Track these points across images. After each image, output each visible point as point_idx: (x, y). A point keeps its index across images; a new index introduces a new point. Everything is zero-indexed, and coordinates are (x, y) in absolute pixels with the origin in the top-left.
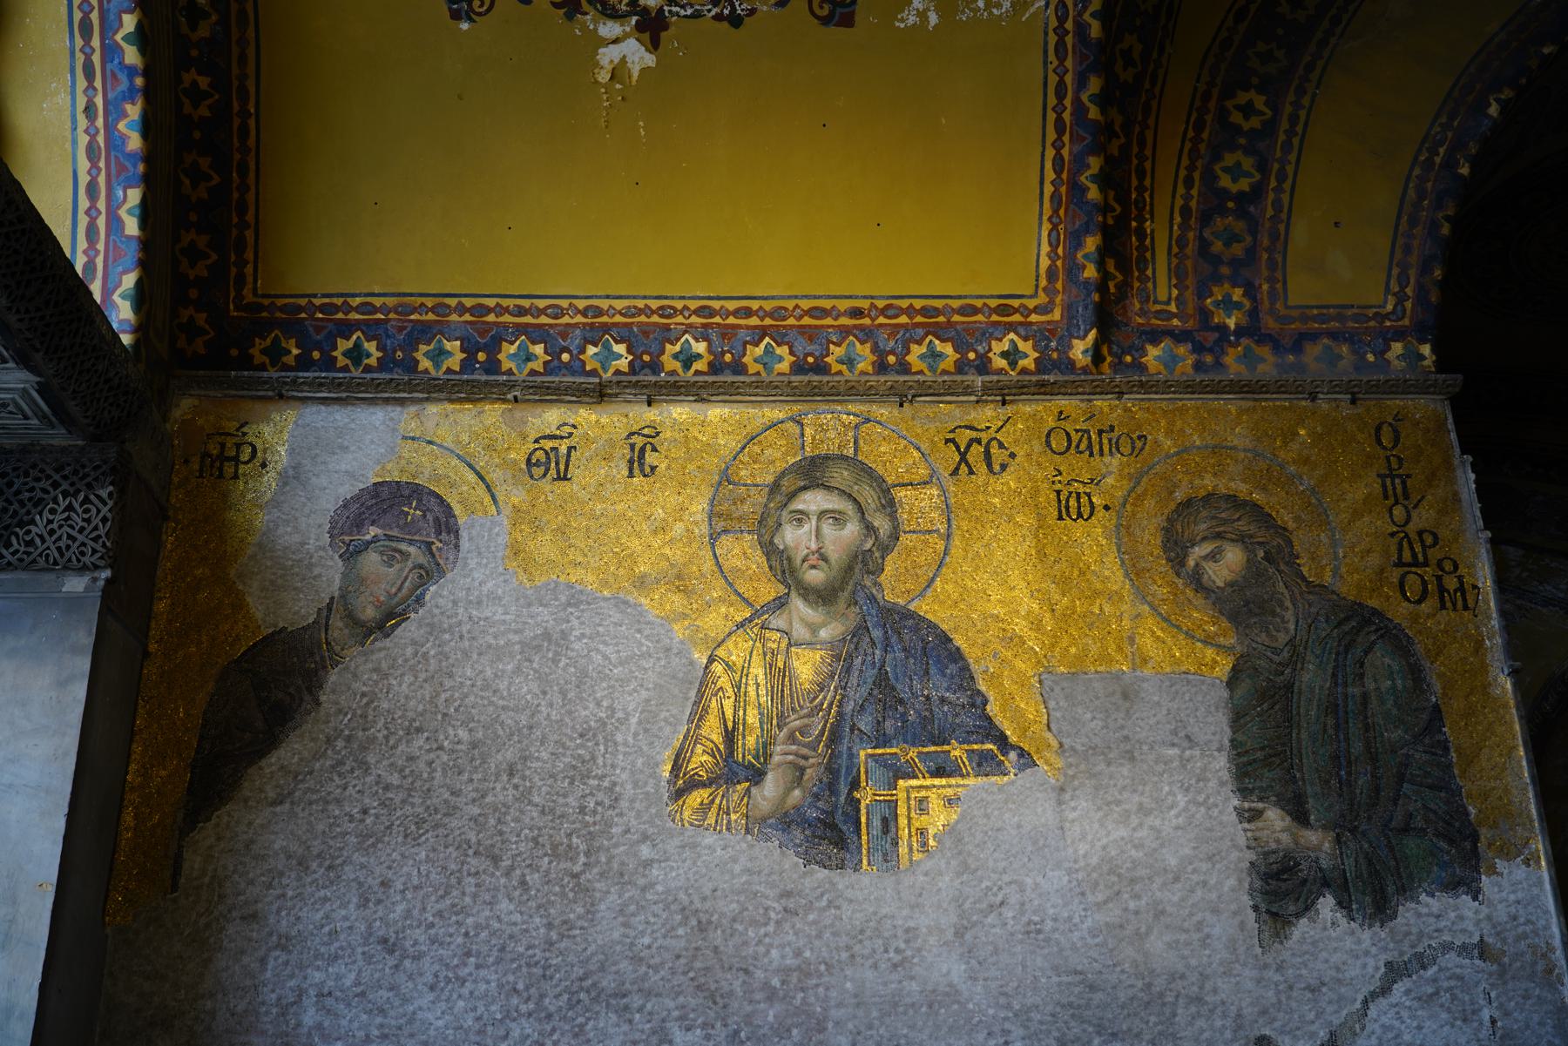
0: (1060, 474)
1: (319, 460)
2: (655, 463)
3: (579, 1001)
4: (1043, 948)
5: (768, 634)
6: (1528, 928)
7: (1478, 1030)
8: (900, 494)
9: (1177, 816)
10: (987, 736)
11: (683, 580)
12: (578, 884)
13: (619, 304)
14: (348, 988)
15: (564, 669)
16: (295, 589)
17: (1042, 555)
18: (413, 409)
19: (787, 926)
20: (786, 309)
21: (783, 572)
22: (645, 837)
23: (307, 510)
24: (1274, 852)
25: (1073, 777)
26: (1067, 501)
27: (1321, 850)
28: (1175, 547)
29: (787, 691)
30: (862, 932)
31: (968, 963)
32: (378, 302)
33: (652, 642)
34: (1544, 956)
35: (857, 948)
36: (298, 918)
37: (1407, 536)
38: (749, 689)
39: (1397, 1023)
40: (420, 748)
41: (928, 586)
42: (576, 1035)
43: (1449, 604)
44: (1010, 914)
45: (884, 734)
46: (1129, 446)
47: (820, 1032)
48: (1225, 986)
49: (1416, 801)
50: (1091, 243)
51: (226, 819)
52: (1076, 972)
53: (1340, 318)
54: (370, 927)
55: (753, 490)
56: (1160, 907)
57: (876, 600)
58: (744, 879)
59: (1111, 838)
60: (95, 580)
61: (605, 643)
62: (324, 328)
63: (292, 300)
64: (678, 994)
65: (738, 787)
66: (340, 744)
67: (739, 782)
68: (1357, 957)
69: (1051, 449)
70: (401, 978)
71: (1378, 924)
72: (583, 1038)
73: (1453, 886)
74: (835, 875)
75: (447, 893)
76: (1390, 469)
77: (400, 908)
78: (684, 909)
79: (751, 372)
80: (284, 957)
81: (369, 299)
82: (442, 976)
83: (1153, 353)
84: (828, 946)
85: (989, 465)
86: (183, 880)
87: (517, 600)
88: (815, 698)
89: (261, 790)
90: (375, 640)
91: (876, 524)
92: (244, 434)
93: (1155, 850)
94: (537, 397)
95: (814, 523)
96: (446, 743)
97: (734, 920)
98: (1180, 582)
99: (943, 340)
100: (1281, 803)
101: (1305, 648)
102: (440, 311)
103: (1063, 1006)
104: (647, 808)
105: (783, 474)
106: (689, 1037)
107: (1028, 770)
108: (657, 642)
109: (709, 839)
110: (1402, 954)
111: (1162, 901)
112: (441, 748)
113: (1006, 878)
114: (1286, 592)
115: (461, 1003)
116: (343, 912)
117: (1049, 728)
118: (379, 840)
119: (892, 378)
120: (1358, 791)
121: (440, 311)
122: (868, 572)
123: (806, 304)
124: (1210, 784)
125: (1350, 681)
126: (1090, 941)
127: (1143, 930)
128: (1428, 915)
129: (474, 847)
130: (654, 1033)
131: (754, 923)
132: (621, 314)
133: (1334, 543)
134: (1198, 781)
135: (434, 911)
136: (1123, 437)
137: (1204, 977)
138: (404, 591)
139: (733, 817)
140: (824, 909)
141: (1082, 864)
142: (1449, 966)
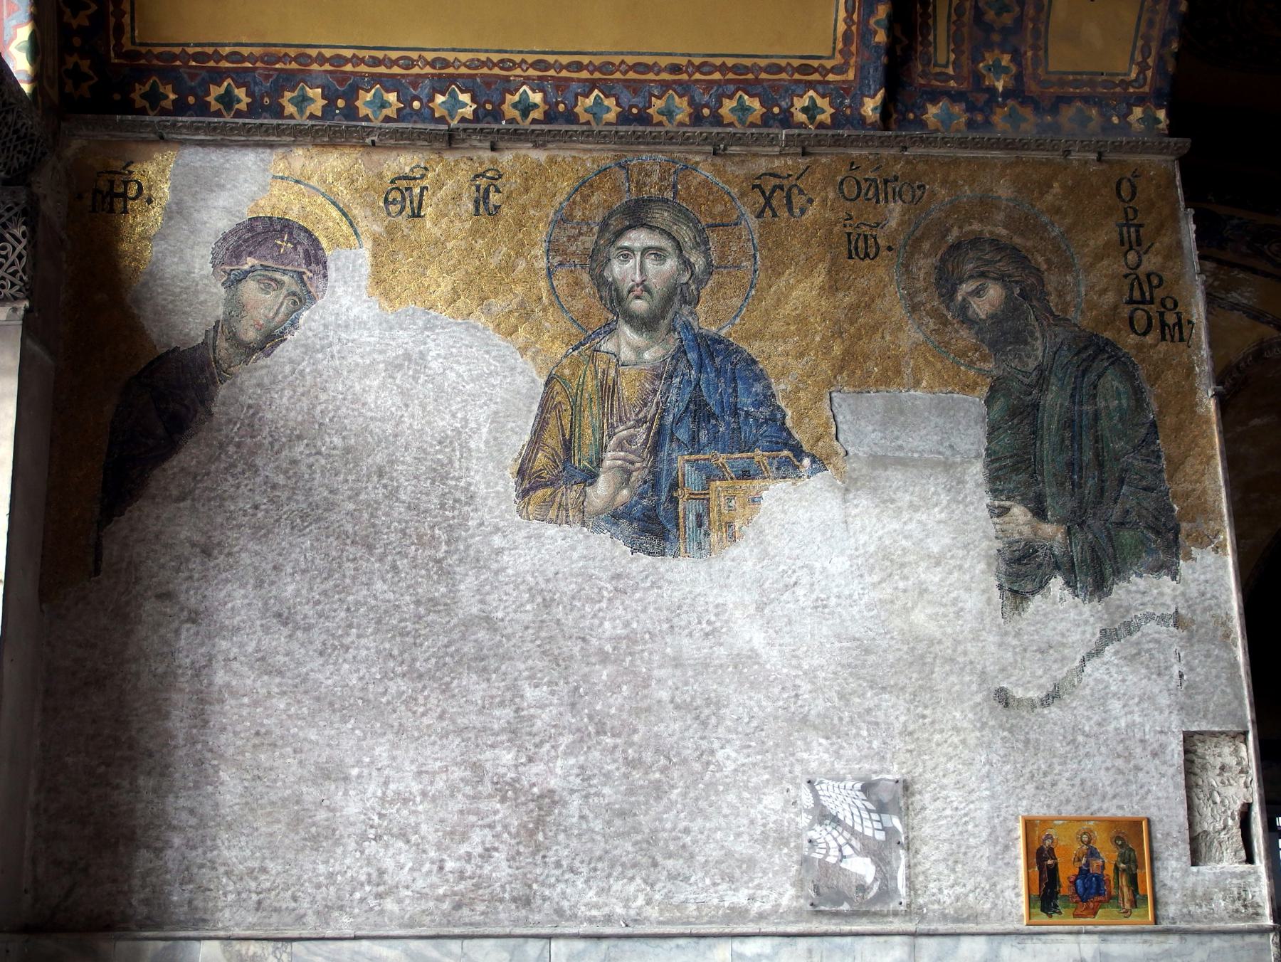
0: (851, 218)
1: (199, 196)
3: (445, 664)
6: (1213, 602)
7: (1169, 682)
9: (941, 512)
10: (786, 445)
12: (441, 568)
13: (464, 57)
14: (251, 654)
15: (423, 385)
16: (184, 313)
17: (833, 287)
18: (280, 151)
19: (617, 603)
20: (613, 64)
21: (612, 301)
22: (497, 529)
23: (190, 242)
25: (856, 480)
26: (857, 241)
28: (946, 282)
30: (680, 607)
32: (245, 51)
34: (1224, 624)
35: (676, 620)
36: (205, 597)
37: (1137, 277)
39: (1106, 677)
40: (301, 453)
42: (443, 692)
43: (1168, 337)
47: (645, 687)
50: (882, 11)
51: (137, 514)
52: (855, 639)
53: (1092, 83)
54: (266, 604)
58: (581, 564)
60: (15, 310)
61: (458, 362)
62: (197, 75)
63: (167, 49)
64: (527, 658)
65: (575, 487)
66: (231, 449)
68: (1079, 626)
69: (842, 192)
70: (295, 646)
72: (448, 694)
73: (1158, 569)
74: (657, 561)
75: (330, 576)
77: (291, 589)
78: (531, 589)
79: (582, 120)
80: (194, 629)
81: (237, 49)
82: (329, 644)
83: (933, 111)
85: (790, 210)
86: (104, 565)
87: (380, 324)
89: (166, 489)
90: (258, 359)
91: (692, 260)
92: (131, 172)
93: (921, 540)
94: (392, 142)
95: (638, 258)
96: (323, 449)
97: (573, 598)
99: (751, 96)
100: (1024, 501)
102: (302, 60)
103: (843, 666)
104: (498, 505)
105: (610, 216)
106: (537, 692)
109: (551, 530)
112: (319, 453)
113: (799, 563)
115: (346, 666)
116: (242, 592)
118: (269, 532)
119: (706, 129)
121: (302, 60)
122: (685, 302)
123: (631, 60)
126: (865, 613)
127: (910, 605)
129: (352, 537)
130: (508, 689)
131: (590, 600)
132: (468, 67)
134: (958, 483)
135: (320, 590)
137: (957, 642)
138: (281, 316)
140: (648, 589)
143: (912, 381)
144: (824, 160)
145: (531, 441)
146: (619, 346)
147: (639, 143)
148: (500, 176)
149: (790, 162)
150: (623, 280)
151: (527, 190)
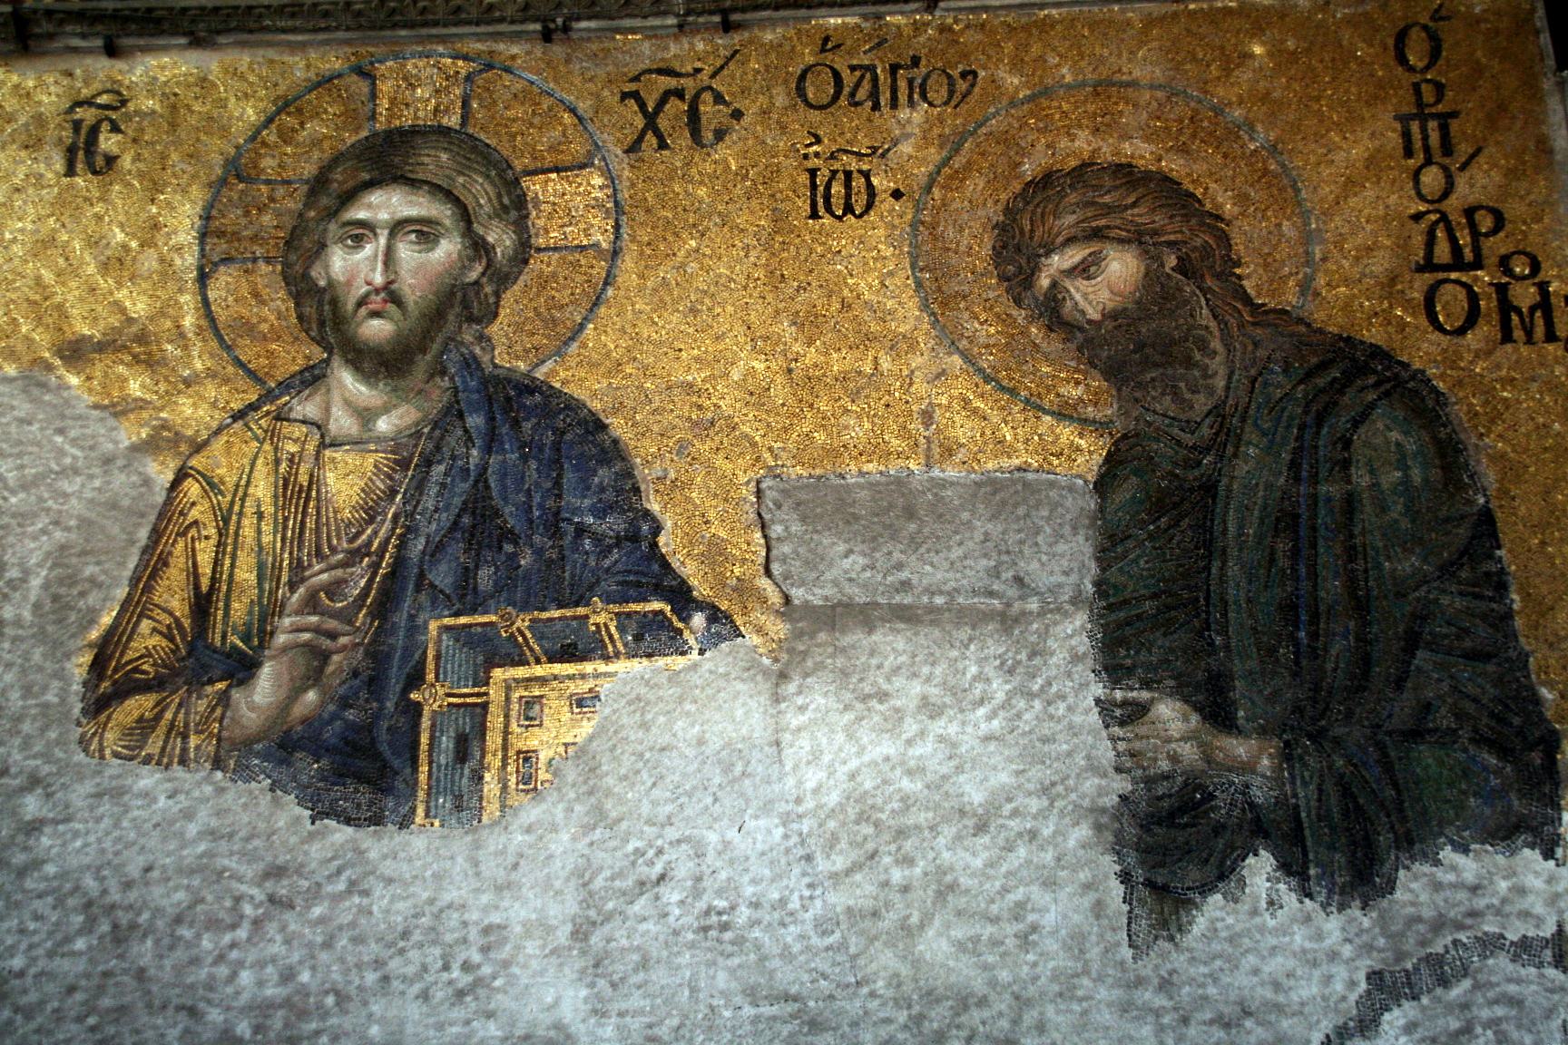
2: (115, 150)
4: (729, 956)
5: (287, 429)
8: (533, 186)
9: (989, 718)
10: (659, 591)
11: (147, 343)
19: (271, 929)
21: (322, 324)
22: (34, 781)
24: (1166, 777)
25: (805, 654)
26: (828, 187)
27: (1253, 772)
29: (310, 523)
30: (405, 935)
31: (592, 985)
33: (82, 448)
35: (394, 964)
37: (1444, 217)
38: (246, 522)
41: (572, 339)
43: (1518, 334)
44: (675, 897)
45: (475, 589)
46: (944, 92)
48: (1060, 1019)
49: (1440, 680)
52: (788, 998)
55: (281, 191)
56: (949, 878)
57: (478, 364)
58: (202, 847)
59: (866, 758)
65: (209, 689)
67: (211, 682)
68: (1315, 964)
71: (1358, 903)
76: (1420, 104)
78: (89, 904)
84: (342, 960)
88: (358, 534)
91: (490, 240)
93: (945, 778)
95: (383, 241)
97: (178, 920)
98: (1020, 315)
100: (1183, 690)
101: (1243, 420)
104: (43, 730)
105: (336, 160)
107: (724, 646)
108: (92, 448)
109: (148, 779)
110: (1400, 956)
111: (952, 869)
113: (672, 833)
114: (1213, 324)
117: (768, 573)
120: (1330, 666)
122: (471, 319)
124: (1055, 659)
125: (1323, 474)
126: (816, 941)
127: (915, 919)
128: (1454, 886)
131: (213, 924)
133: (1307, 238)
134: (1030, 658)
136: (934, 76)
137: (1021, 1002)
139: (193, 741)
140: (337, 898)
141: (809, 804)
142: (1494, 979)
143: (936, 450)
144: (768, 36)
145: (129, 596)
146: (327, 410)
147: (395, 26)
148: (124, 103)
149: (700, 46)
150: (349, 283)
151: (173, 126)
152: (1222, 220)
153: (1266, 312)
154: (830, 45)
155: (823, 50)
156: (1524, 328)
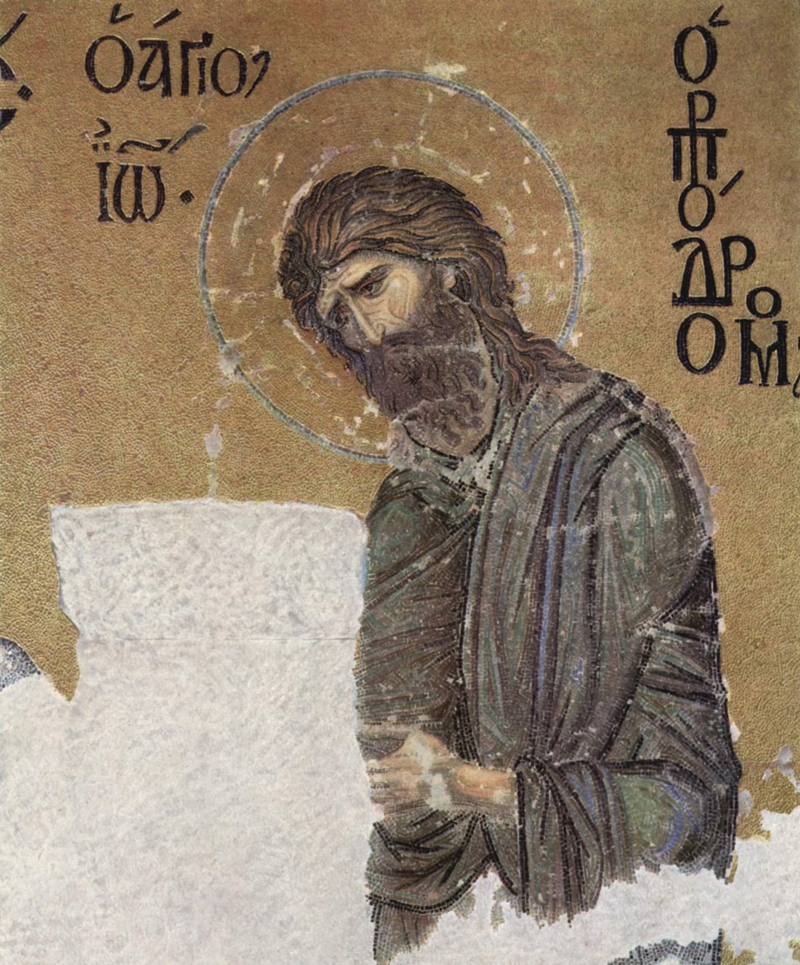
37: (703, 247)
43: (756, 375)
76: (692, 119)
152: (500, 237)
153: (533, 342)
154: (119, 16)
155: (113, 21)
156: (761, 369)
